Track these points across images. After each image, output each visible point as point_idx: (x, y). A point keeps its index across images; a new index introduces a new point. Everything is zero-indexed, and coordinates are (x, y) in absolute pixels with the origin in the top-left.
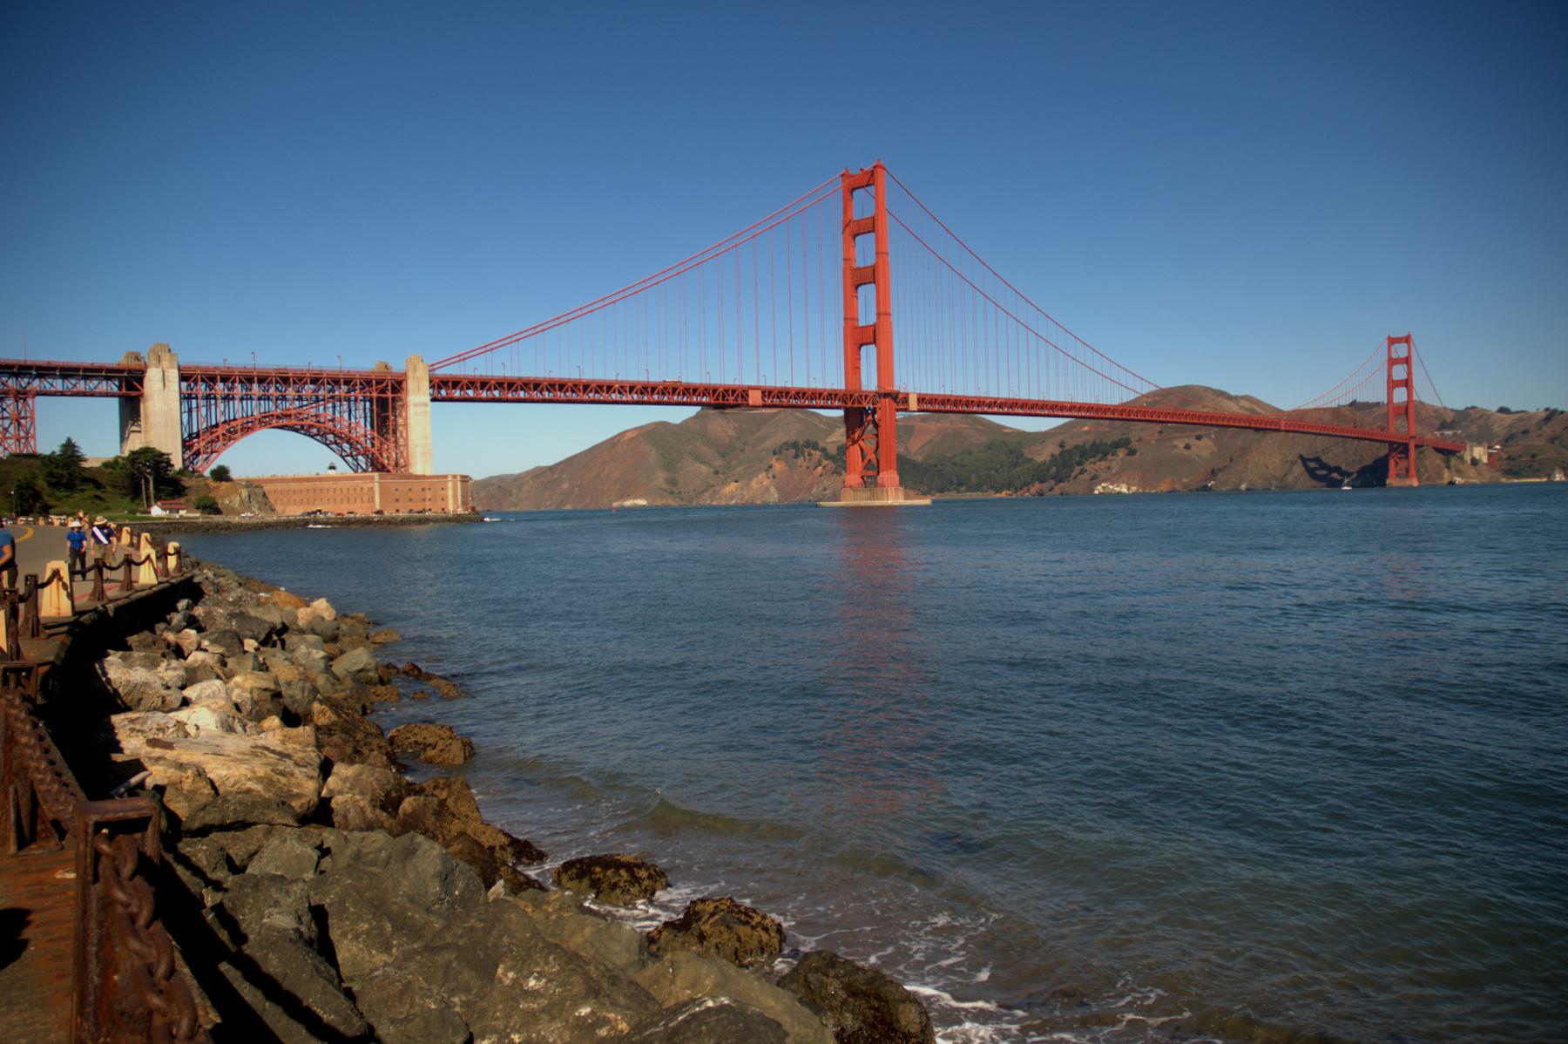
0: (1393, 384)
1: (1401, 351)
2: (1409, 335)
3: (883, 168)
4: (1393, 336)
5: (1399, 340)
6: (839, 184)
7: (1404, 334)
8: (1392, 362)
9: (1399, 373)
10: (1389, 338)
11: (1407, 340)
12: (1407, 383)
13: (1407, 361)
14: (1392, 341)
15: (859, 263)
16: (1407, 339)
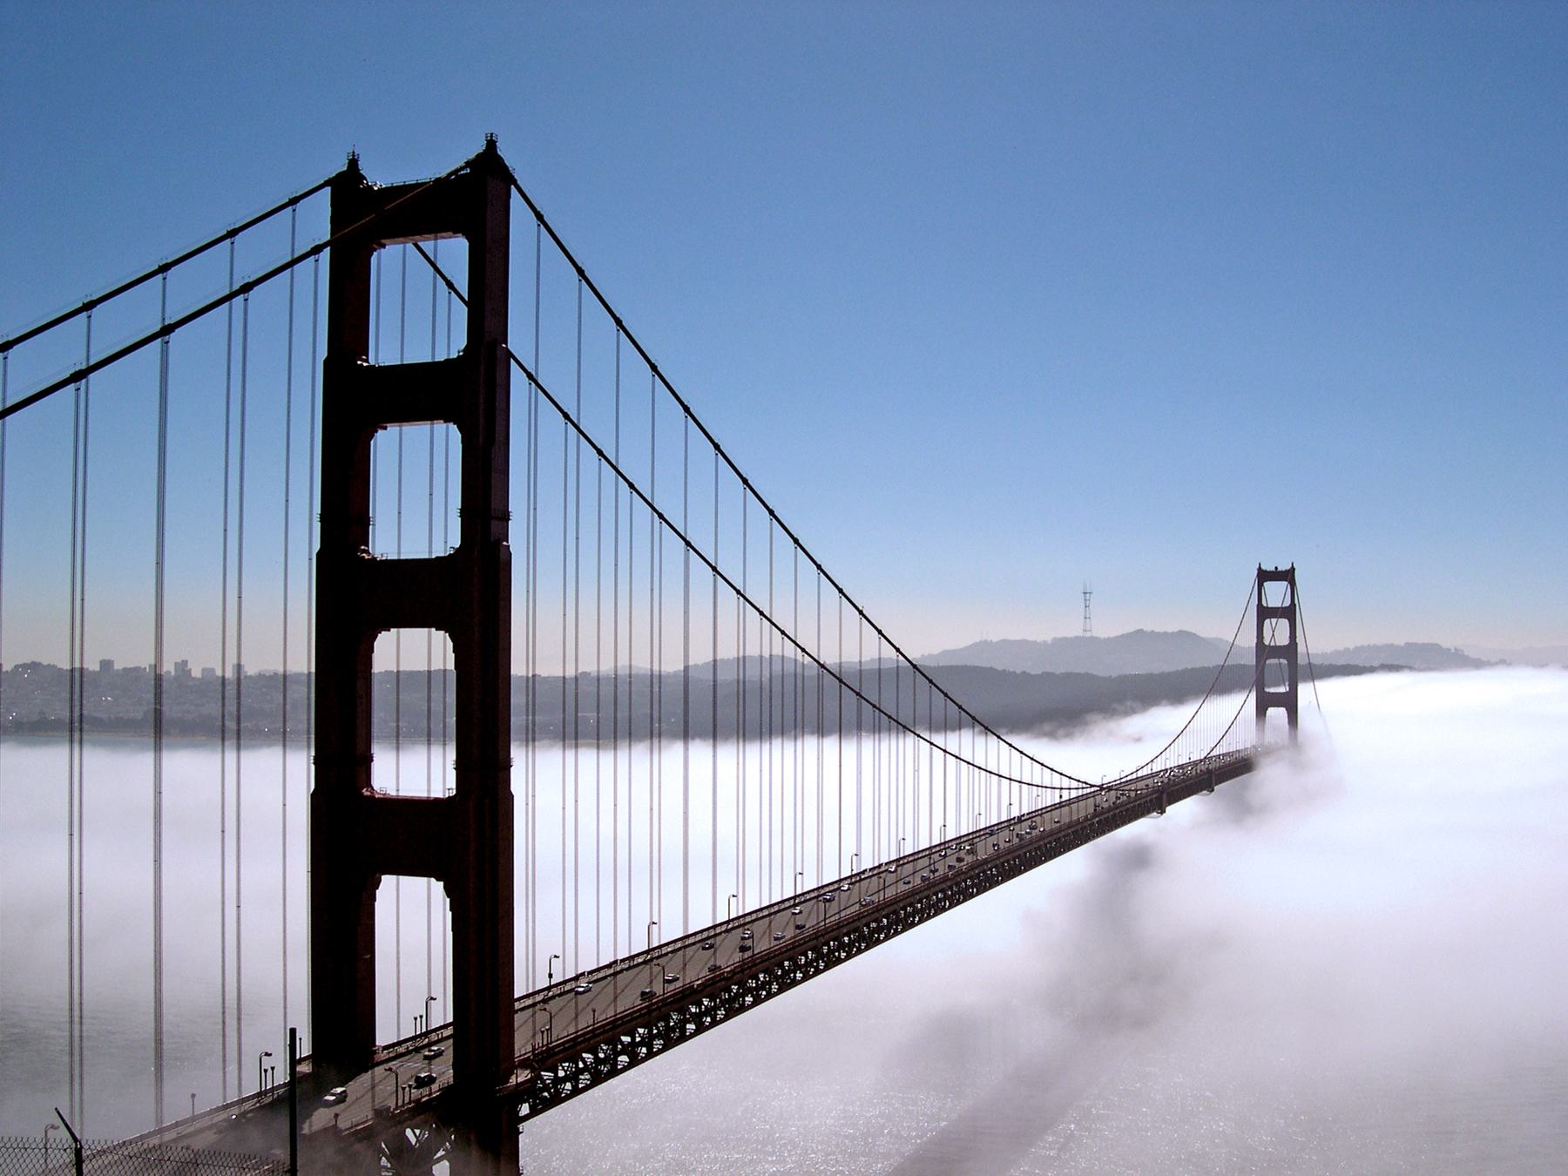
0: (1263, 651)
1: (1276, 594)
2: (1293, 569)
3: (506, 178)
4: (1269, 567)
5: (1276, 575)
6: (319, 211)
7: (1279, 569)
8: (1264, 613)
9: (1278, 633)
10: (1260, 569)
11: (1288, 576)
12: (1290, 650)
13: (1289, 613)
14: (1264, 576)
15: (385, 543)
16: (1288, 576)
